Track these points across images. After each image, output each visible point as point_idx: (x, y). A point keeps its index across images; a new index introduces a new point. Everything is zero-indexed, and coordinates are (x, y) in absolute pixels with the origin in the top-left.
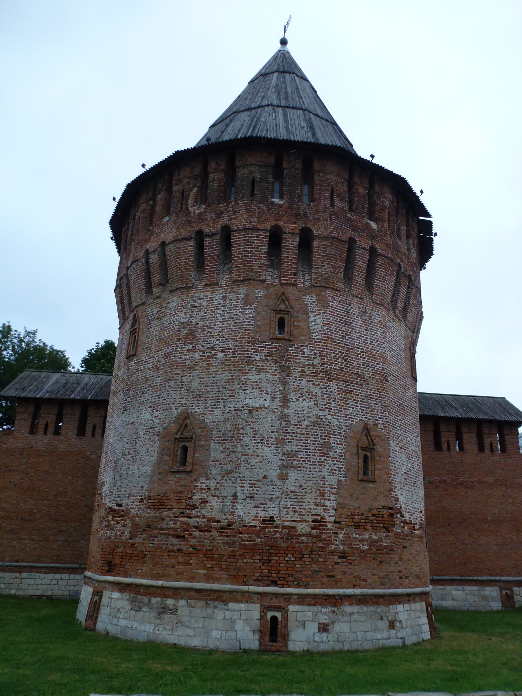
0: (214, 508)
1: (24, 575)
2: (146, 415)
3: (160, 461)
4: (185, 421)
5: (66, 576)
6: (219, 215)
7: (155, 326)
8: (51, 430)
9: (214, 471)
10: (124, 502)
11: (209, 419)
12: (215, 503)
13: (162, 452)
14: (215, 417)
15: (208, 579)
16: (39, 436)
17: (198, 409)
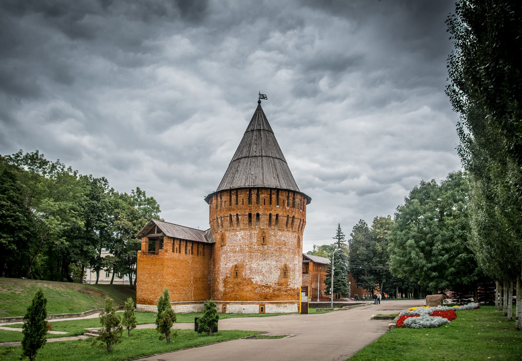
0: (291, 286)
1: (177, 306)
2: (274, 263)
3: (281, 275)
4: (286, 266)
5: (187, 305)
6: (292, 212)
7: (273, 237)
8: (178, 251)
9: (291, 278)
10: (269, 284)
11: (290, 266)
12: (292, 284)
13: (281, 274)
14: (291, 266)
15: (291, 300)
16: (175, 253)
17: (288, 264)
